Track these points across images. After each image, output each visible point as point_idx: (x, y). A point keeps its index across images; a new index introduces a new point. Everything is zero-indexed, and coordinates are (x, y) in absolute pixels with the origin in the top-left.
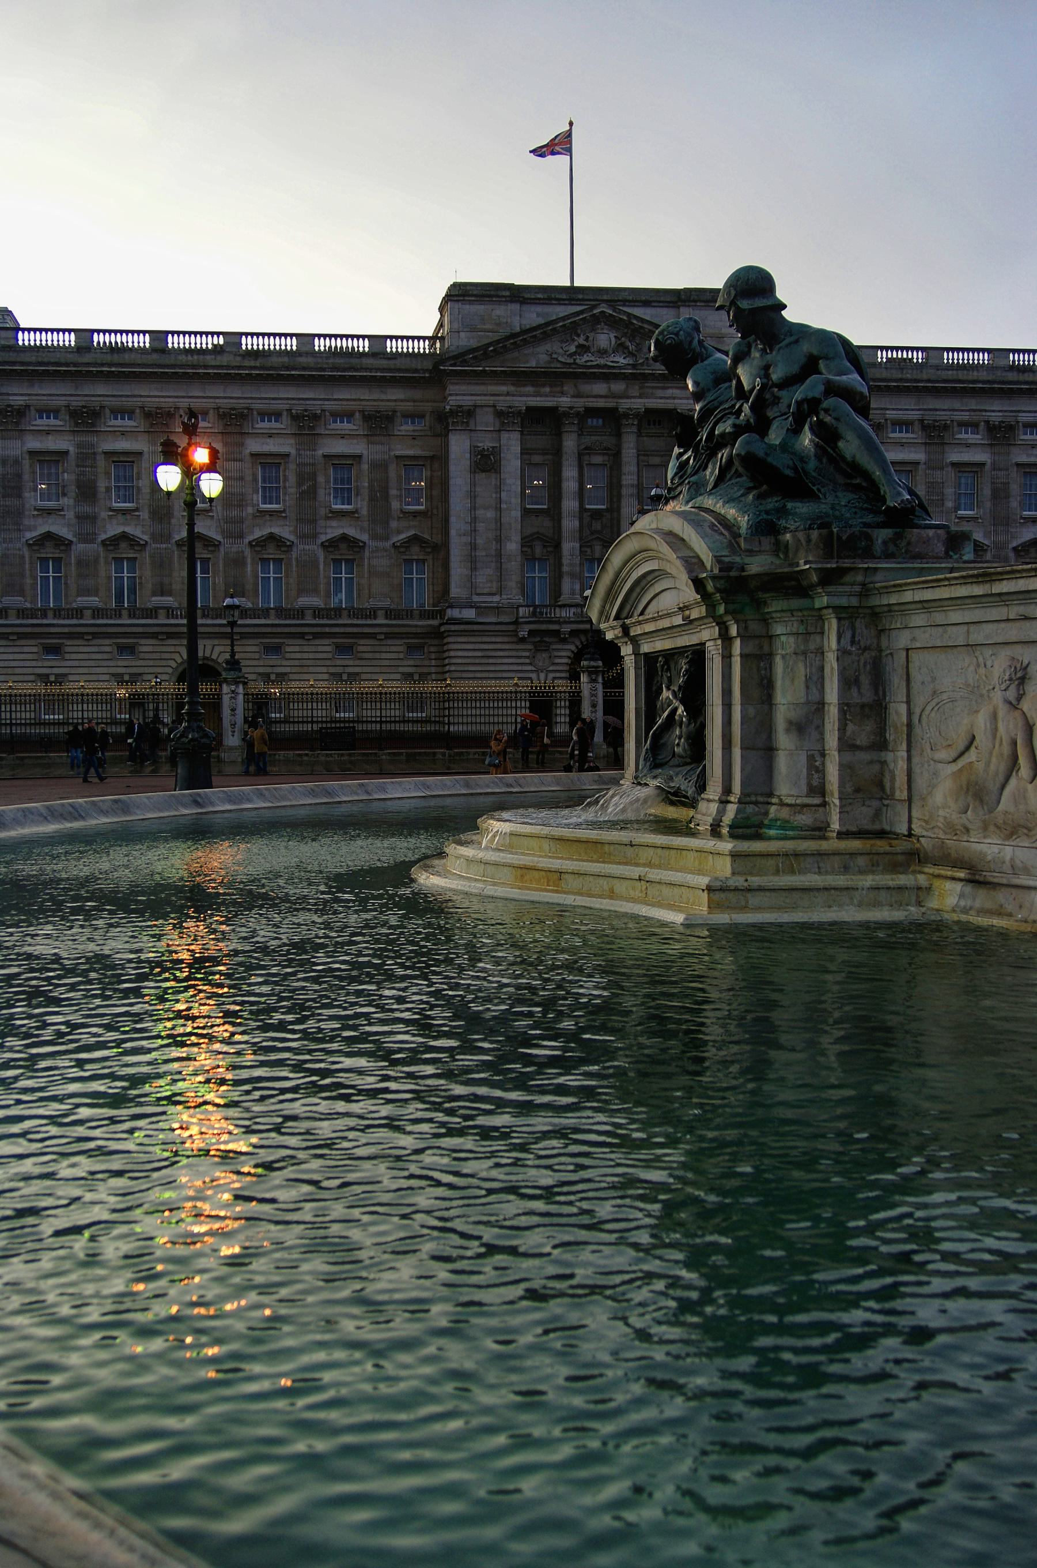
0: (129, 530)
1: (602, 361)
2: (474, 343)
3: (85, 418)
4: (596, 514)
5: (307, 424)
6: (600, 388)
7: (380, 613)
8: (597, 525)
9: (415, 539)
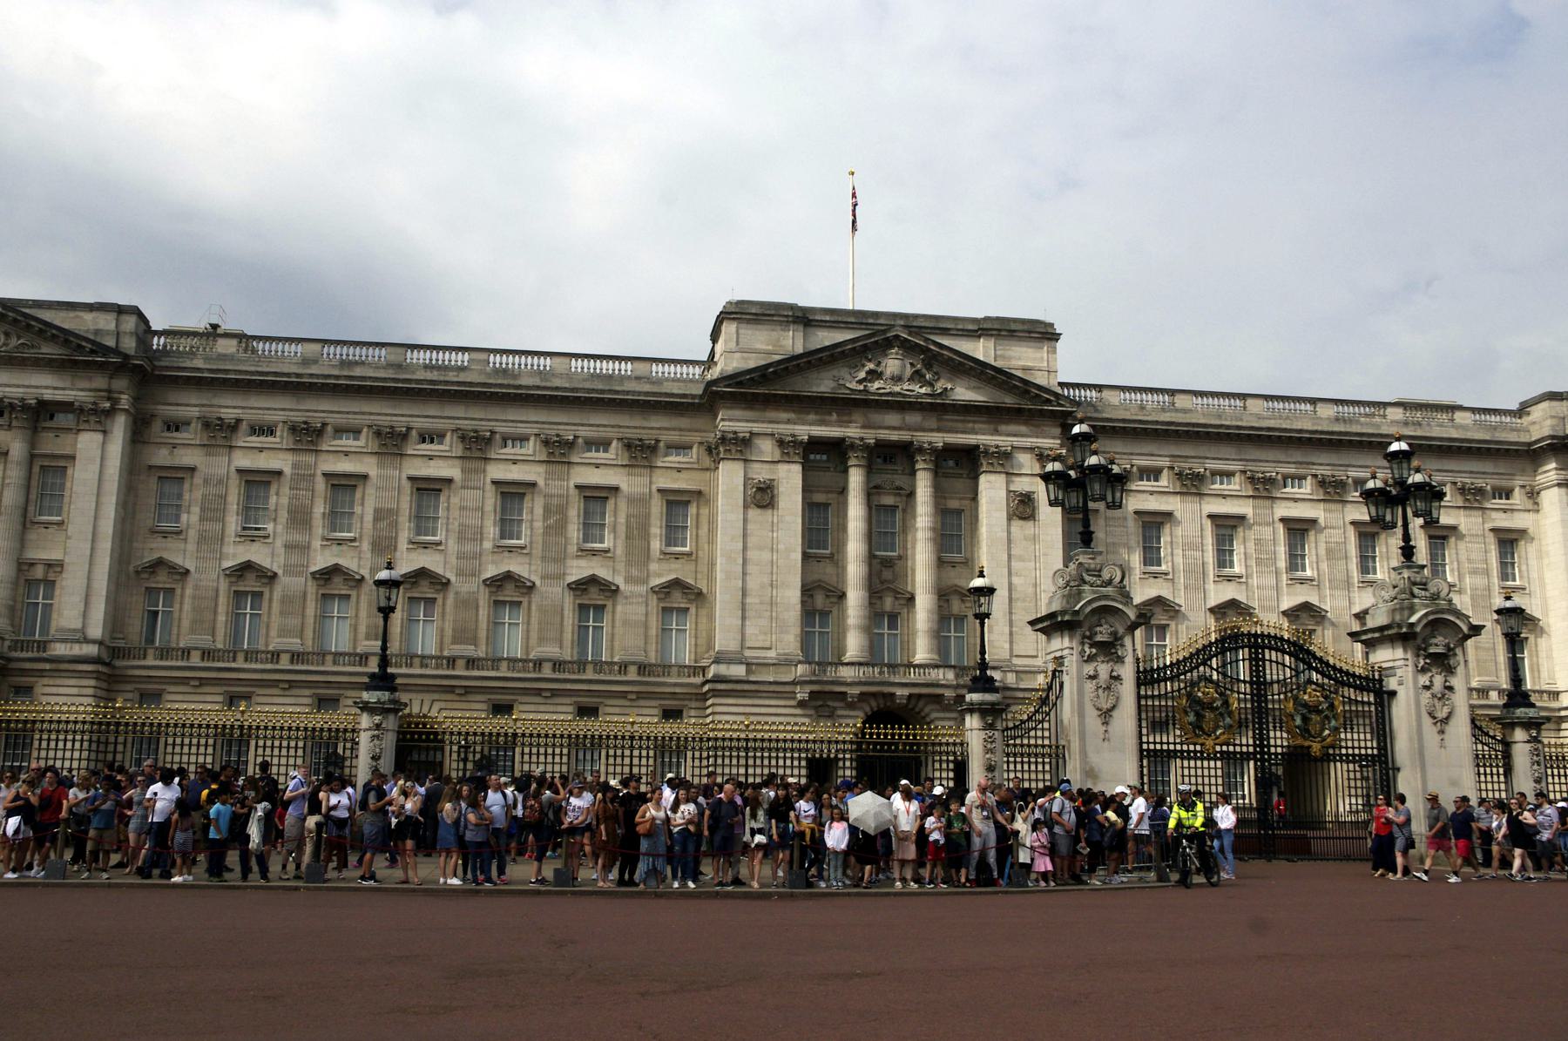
0: (341, 562)
1: (897, 389)
2: (752, 364)
3: (307, 436)
4: (888, 563)
5: (559, 451)
6: (892, 418)
7: (633, 669)
8: (887, 574)
9: (677, 584)
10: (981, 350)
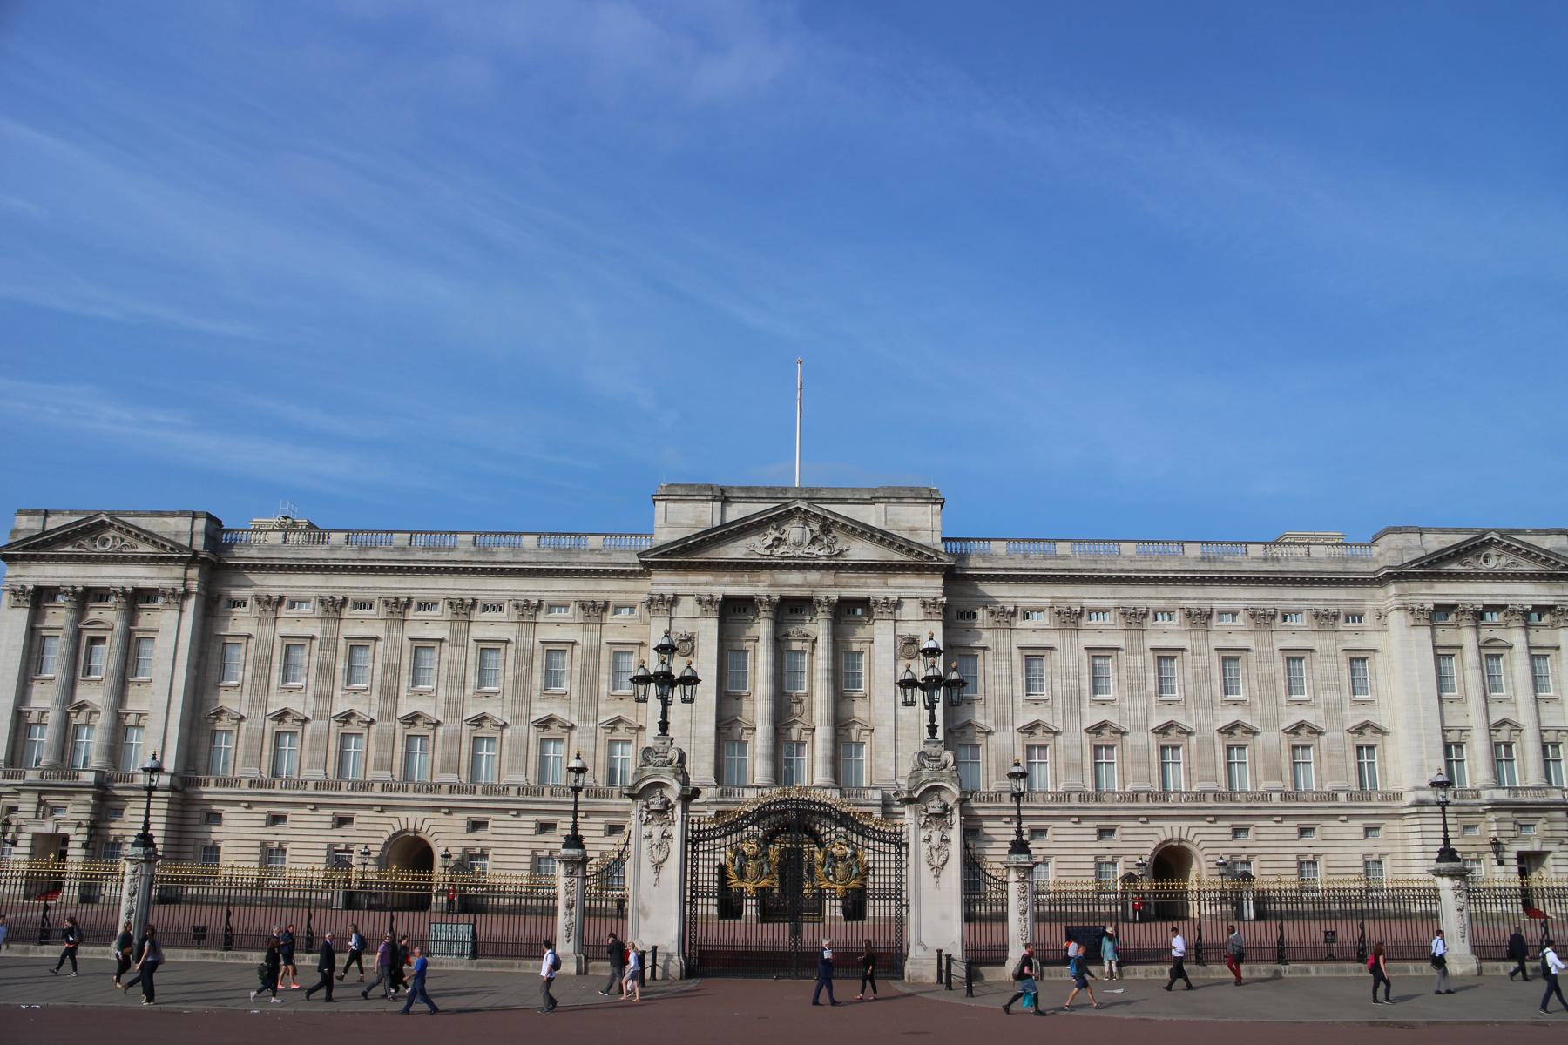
0: (357, 708)
1: (799, 553)
2: (677, 537)
6: (795, 577)
10: (871, 515)
